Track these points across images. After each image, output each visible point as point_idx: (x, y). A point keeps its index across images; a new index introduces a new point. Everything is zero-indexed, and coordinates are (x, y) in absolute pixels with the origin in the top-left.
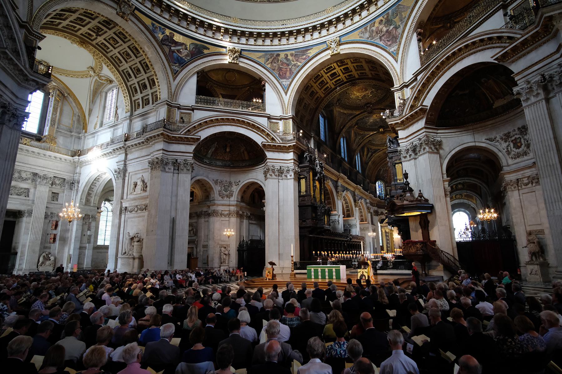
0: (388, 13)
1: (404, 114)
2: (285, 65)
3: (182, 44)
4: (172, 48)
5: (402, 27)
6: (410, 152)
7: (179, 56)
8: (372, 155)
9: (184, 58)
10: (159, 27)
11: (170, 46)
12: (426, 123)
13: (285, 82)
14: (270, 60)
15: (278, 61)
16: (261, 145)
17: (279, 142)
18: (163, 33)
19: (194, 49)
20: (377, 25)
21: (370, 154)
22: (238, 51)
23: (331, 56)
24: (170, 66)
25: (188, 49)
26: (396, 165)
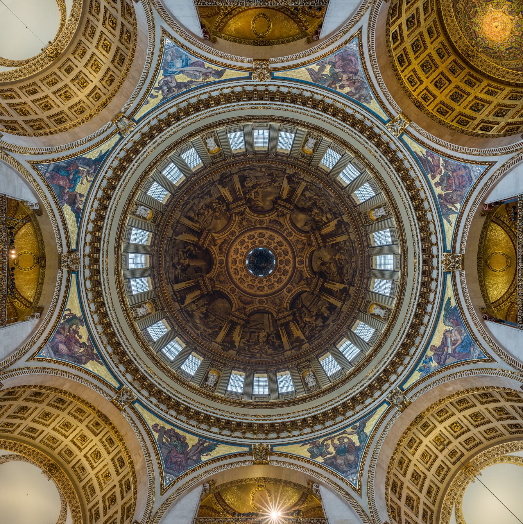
3: (445, 337)
4: (450, 352)
5: (328, 60)
7: (460, 344)
9: (463, 337)
10: (423, 363)
11: (447, 354)
18: (431, 360)
19: (451, 320)
22: (446, 256)
24: (472, 362)
25: (451, 328)
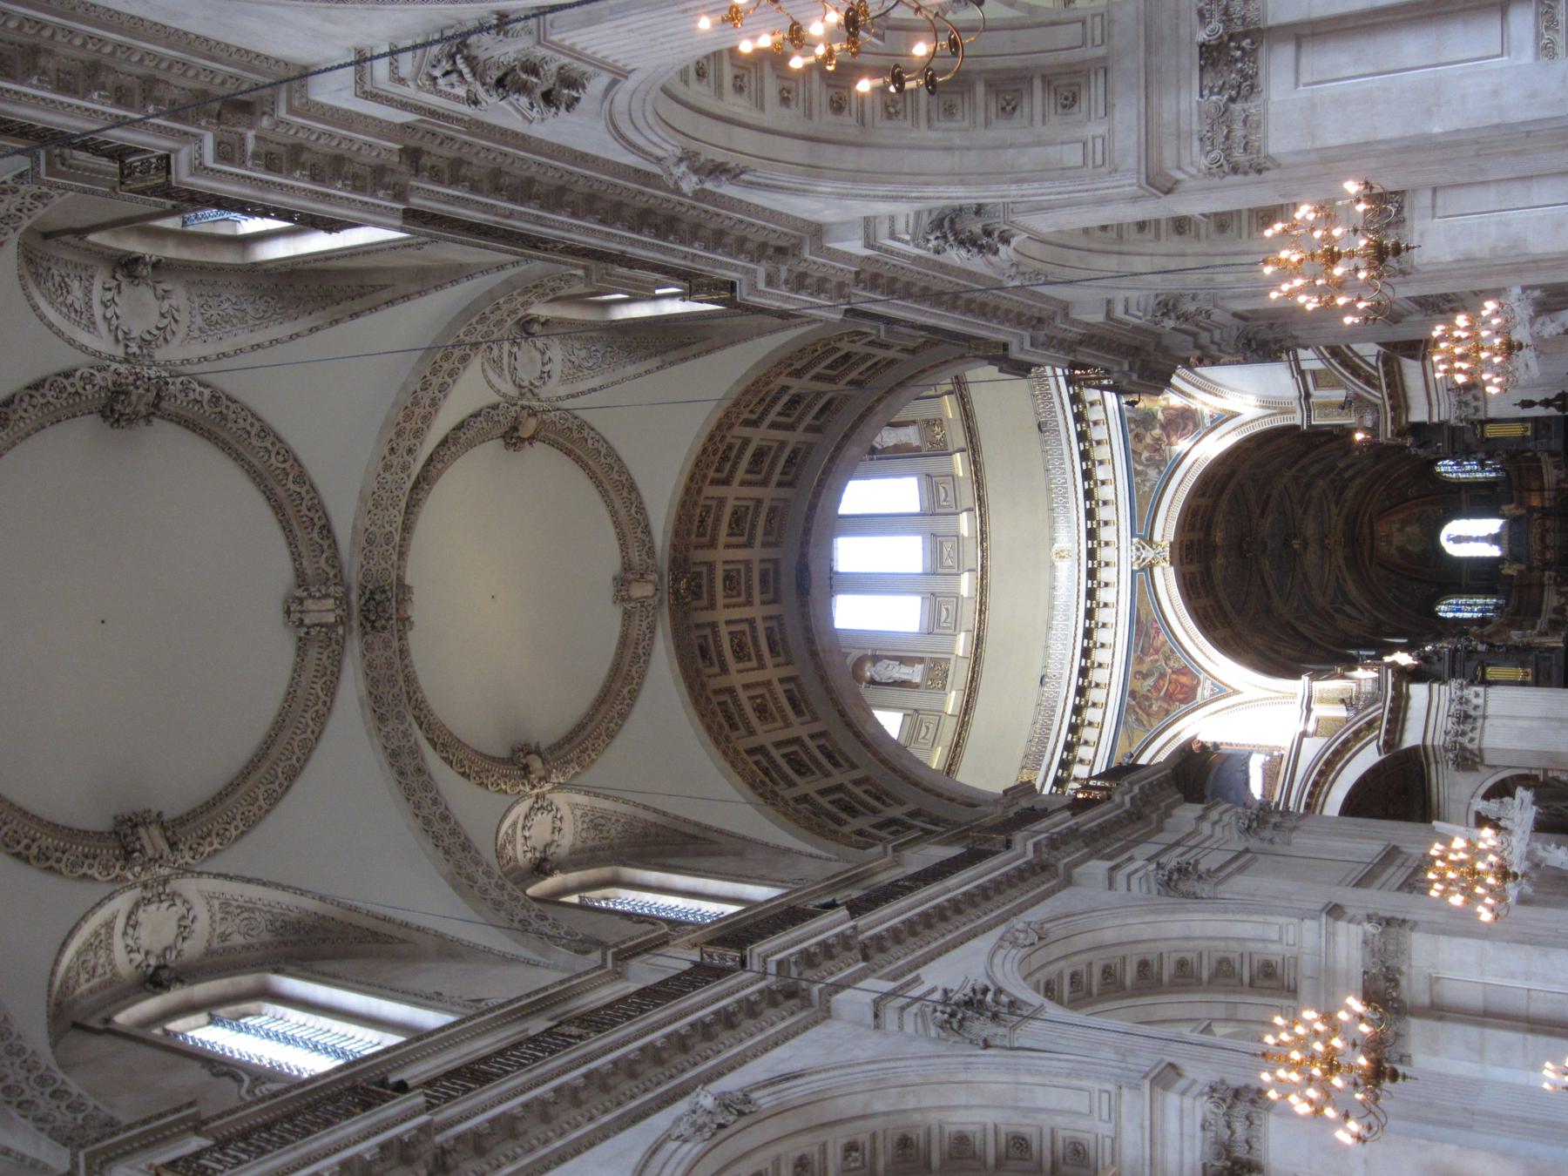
0: (1130, 419)
1: (1379, 402)
2: (1161, 683)
6: (1469, 398)
8: (1353, 605)
12: (1413, 357)
13: (1204, 691)
14: (1144, 717)
15: (1147, 698)
16: (1383, 756)
17: (1382, 711)
20: (1140, 447)
21: (1347, 608)
23: (1171, 564)
26: (1488, 435)
